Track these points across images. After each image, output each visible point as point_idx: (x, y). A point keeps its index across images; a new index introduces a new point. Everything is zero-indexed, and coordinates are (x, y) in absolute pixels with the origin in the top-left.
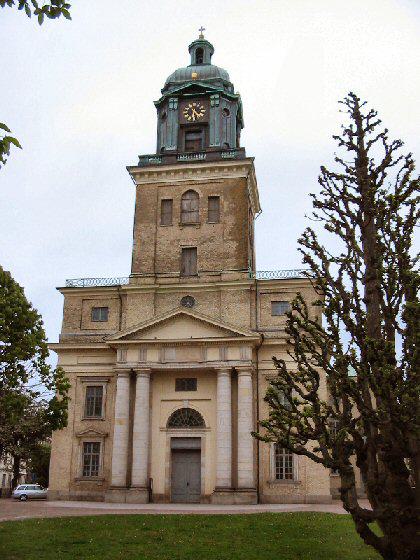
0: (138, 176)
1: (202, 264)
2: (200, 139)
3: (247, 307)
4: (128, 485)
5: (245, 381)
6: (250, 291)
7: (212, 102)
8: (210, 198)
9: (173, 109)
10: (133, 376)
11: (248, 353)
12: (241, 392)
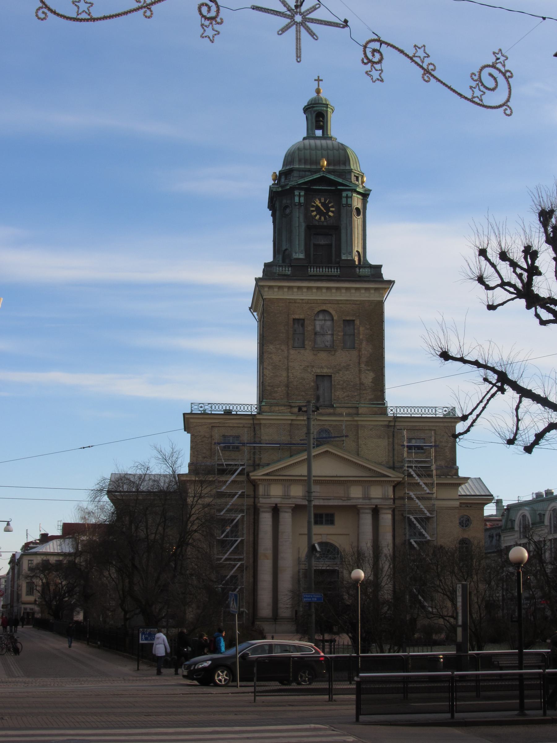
0: (266, 289)
1: (339, 393)
2: (330, 245)
3: (384, 443)
4: (275, 618)
5: (386, 518)
6: (388, 426)
7: (344, 201)
8: (344, 320)
9: (300, 203)
10: (276, 511)
11: (390, 493)
12: (381, 530)
